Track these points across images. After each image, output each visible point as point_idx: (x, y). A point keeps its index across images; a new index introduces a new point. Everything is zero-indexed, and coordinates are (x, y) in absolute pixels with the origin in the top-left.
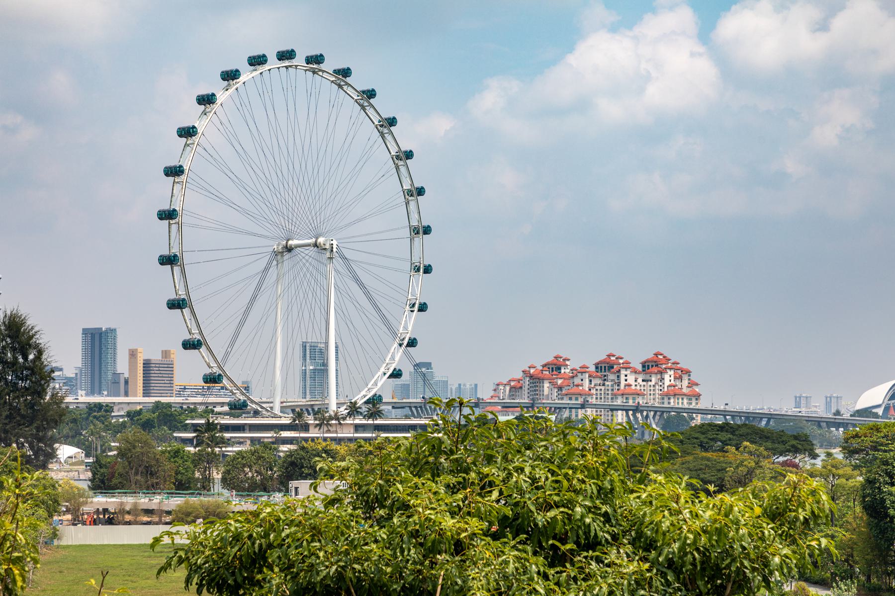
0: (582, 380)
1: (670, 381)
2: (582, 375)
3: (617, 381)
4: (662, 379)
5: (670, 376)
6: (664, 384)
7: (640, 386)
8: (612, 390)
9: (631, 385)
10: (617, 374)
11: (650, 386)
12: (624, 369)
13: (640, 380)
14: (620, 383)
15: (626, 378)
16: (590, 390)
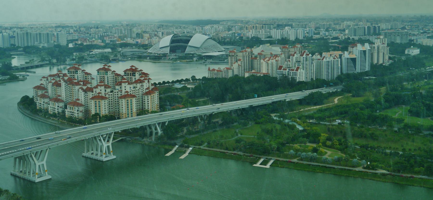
0: (101, 90)
2: (101, 88)
3: (120, 90)
4: (142, 86)
6: (143, 88)
7: (132, 91)
8: (118, 95)
9: (128, 92)
11: (137, 90)
12: (124, 84)
13: (132, 88)
14: (122, 91)
15: (125, 88)
16: (105, 95)
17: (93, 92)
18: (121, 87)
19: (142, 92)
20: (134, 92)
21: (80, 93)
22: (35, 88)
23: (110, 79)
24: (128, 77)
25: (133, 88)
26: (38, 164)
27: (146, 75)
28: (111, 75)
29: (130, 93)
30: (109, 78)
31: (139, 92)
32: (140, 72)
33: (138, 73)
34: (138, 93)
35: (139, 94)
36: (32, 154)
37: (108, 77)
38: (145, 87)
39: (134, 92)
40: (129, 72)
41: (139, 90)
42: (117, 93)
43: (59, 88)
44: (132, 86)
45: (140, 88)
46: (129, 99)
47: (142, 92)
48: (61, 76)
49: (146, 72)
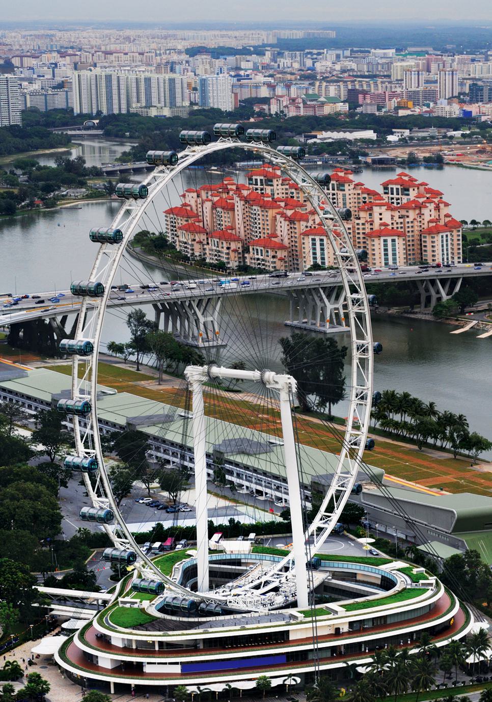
1: (431, 215)
3: (369, 220)
4: (420, 215)
5: (430, 211)
6: (423, 219)
7: (397, 223)
9: (388, 225)
10: (368, 212)
11: (408, 222)
13: (396, 218)
14: (373, 221)
15: (381, 217)
17: (307, 221)
18: (370, 215)
19: (421, 226)
20: (402, 225)
21: (279, 225)
22: (170, 211)
23: (350, 199)
24: (392, 196)
25: (399, 218)
26: (202, 319)
27: (438, 194)
28: (352, 191)
29: (393, 228)
30: (348, 197)
31: (412, 227)
32: (422, 188)
33: (416, 189)
34: (410, 229)
35: (412, 231)
36: (192, 302)
37: (344, 195)
38: (427, 218)
39: (402, 225)
40: (395, 187)
41: (412, 222)
42: (363, 227)
43: (228, 213)
44: (396, 214)
45: (415, 219)
46: (389, 239)
47: (421, 226)
48: (232, 190)
49: (435, 189)
